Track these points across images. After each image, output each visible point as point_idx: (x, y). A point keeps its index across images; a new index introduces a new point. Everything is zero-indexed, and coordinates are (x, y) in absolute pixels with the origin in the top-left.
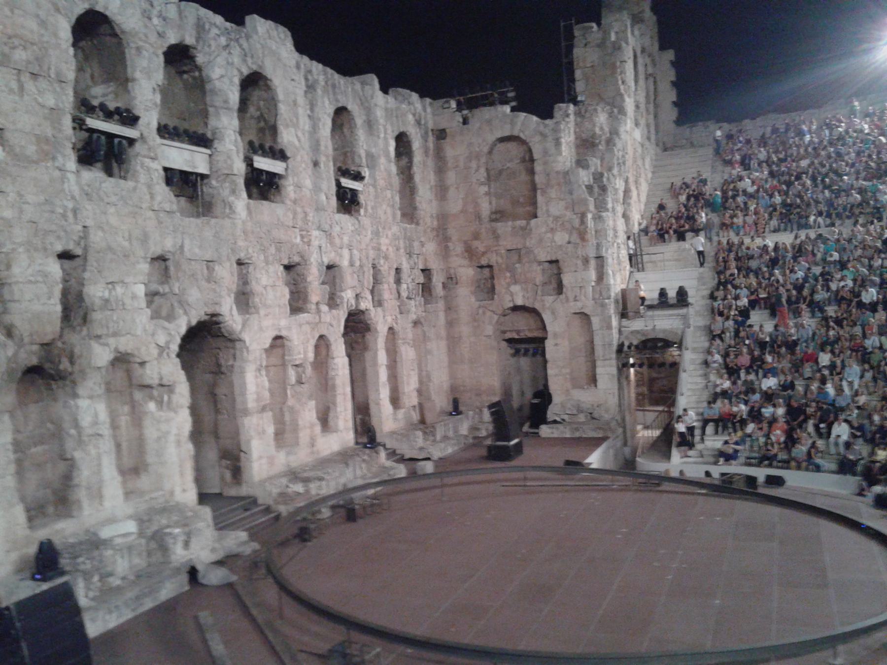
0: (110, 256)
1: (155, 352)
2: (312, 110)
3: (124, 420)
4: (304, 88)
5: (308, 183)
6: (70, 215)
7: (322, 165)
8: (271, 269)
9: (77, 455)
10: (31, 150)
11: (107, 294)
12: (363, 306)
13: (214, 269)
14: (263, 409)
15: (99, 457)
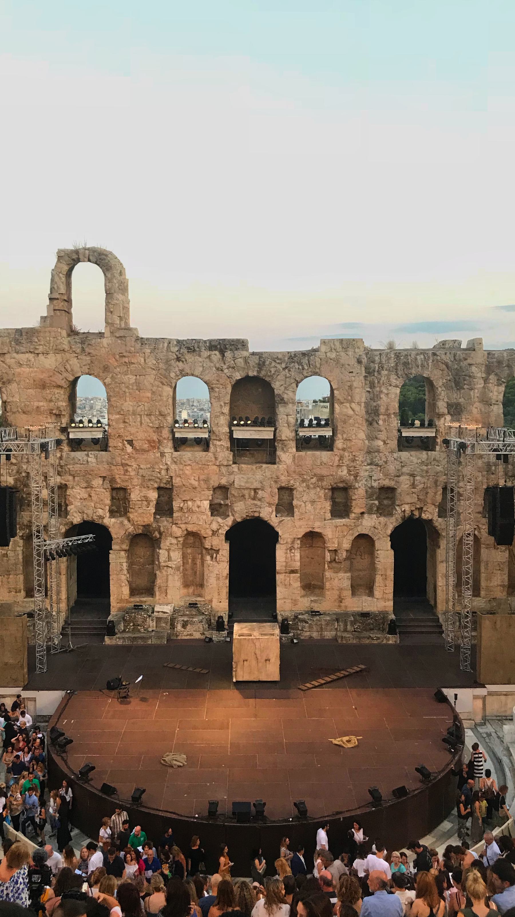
0: (184, 488)
1: (210, 533)
2: (372, 386)
3: (198, 562)
4: (364, 374)
5: (362, 435)
6: (163, 472)
7: (381, 422)
8: (313, 492)
9: (158, 572)
10: (146, 446)
11: (182, 505)
12: (424, 516)
13: (258, 493)
14: (293, 572)
15: (167, 576)
